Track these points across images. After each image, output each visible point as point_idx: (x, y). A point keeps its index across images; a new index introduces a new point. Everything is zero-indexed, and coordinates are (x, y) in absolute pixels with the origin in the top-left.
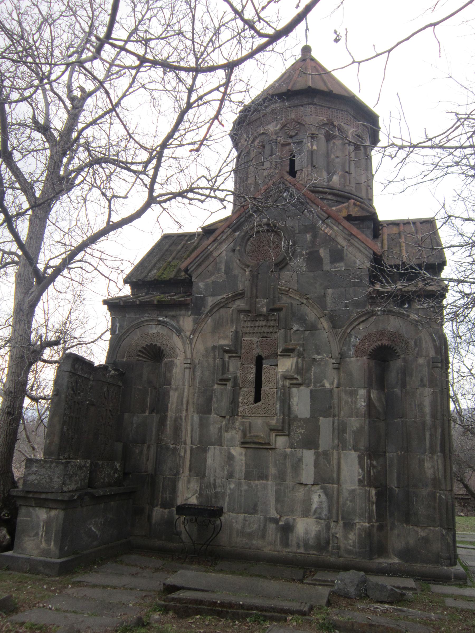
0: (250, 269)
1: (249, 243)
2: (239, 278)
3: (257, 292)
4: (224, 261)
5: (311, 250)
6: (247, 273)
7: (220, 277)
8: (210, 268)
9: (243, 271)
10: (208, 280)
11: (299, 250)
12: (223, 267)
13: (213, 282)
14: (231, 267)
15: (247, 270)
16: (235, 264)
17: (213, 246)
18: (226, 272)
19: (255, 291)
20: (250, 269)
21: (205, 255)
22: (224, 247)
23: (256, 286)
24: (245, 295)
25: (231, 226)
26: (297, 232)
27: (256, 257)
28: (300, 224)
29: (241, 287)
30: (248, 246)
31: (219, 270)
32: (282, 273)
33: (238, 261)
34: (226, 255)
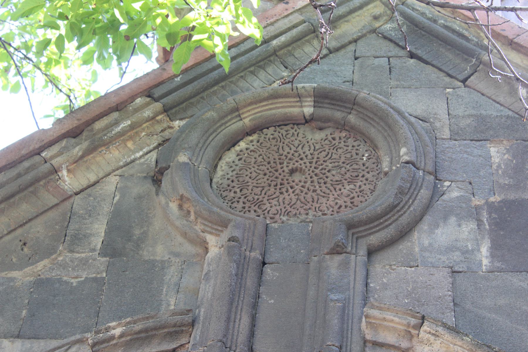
0: (226, 235)
1: (230, 156)
2: (171, 274)
3: (252, 334)
4: (106, 208)
5: (512, 196)
6: (214, 251)
7: (82, 265)
8: (38, 229)
9: (189, 248)
10: (15, 274)
11: (455, 194)
12: (99, 230)
13: (40, 283)
14: (137, 232)
15: (211, 240)
16: (157, 224)
17: (66, 149)
18: (110, 250)
19: (245, 321)
20: (226, 235)
21: (28, 177)
22: (114, 155)
23: (255, 306)
24: (197, 333)
25: (157, 92)
26: (447, 134)
27: (259, 204)
28: (460, 112)
29: (171, 303)
30: (223, 165)
31: (78, 240)
32: (378, 268)
33: (174, 206)
34: (122, 190)
